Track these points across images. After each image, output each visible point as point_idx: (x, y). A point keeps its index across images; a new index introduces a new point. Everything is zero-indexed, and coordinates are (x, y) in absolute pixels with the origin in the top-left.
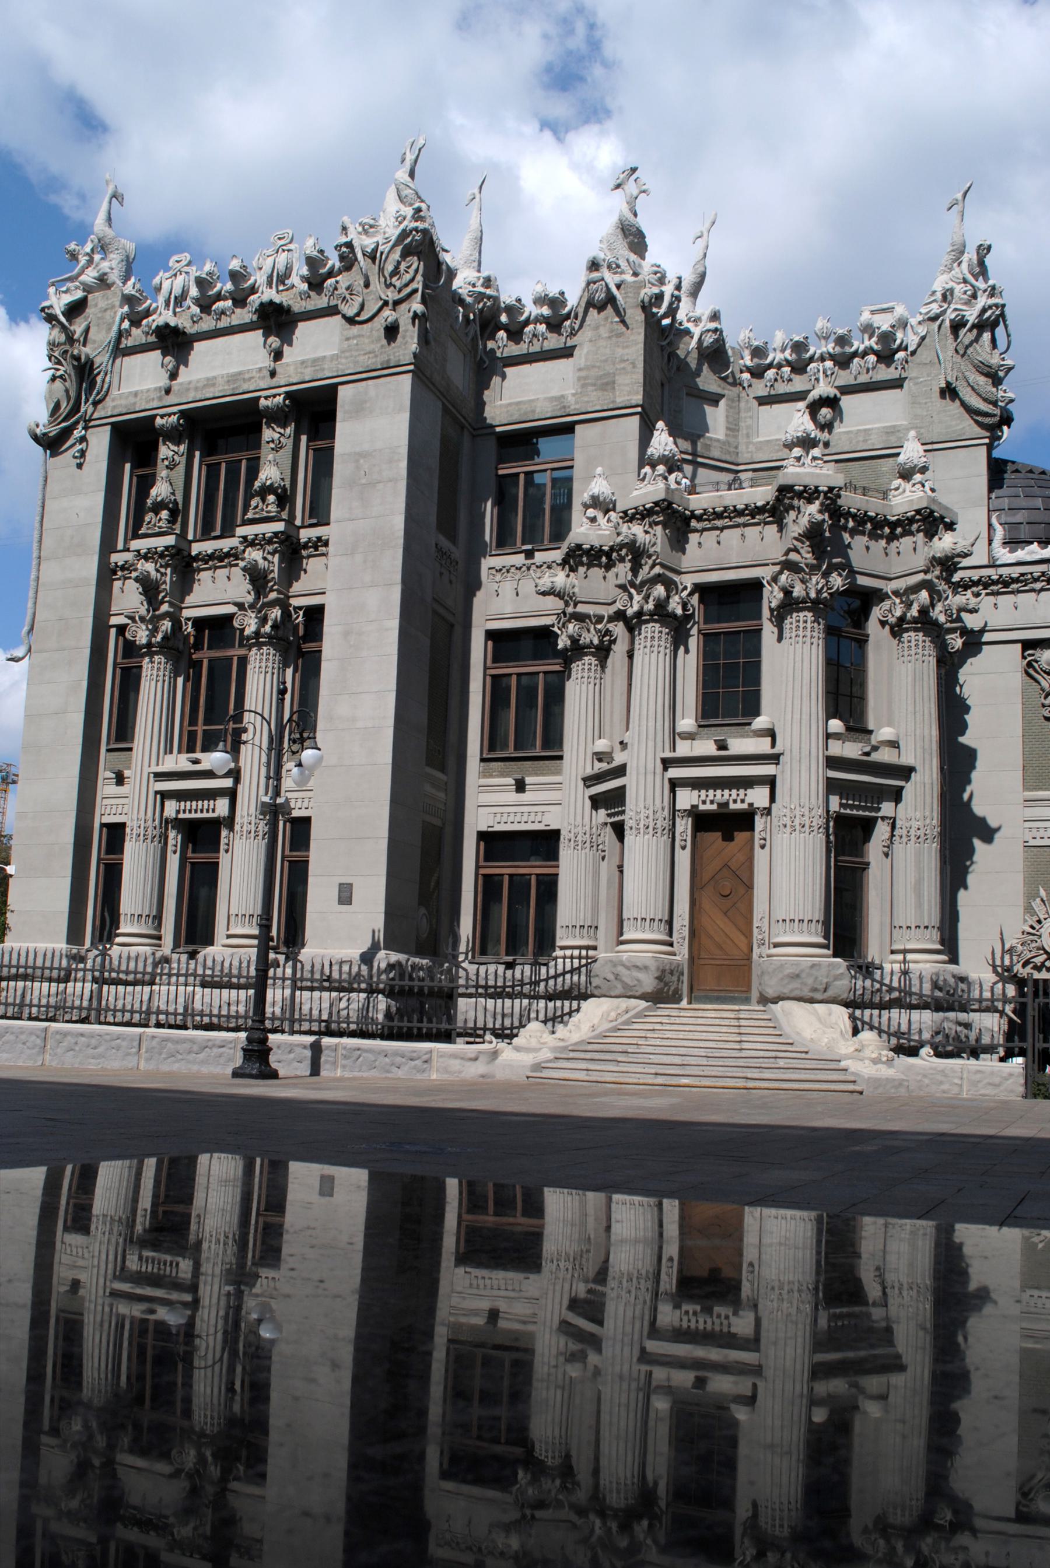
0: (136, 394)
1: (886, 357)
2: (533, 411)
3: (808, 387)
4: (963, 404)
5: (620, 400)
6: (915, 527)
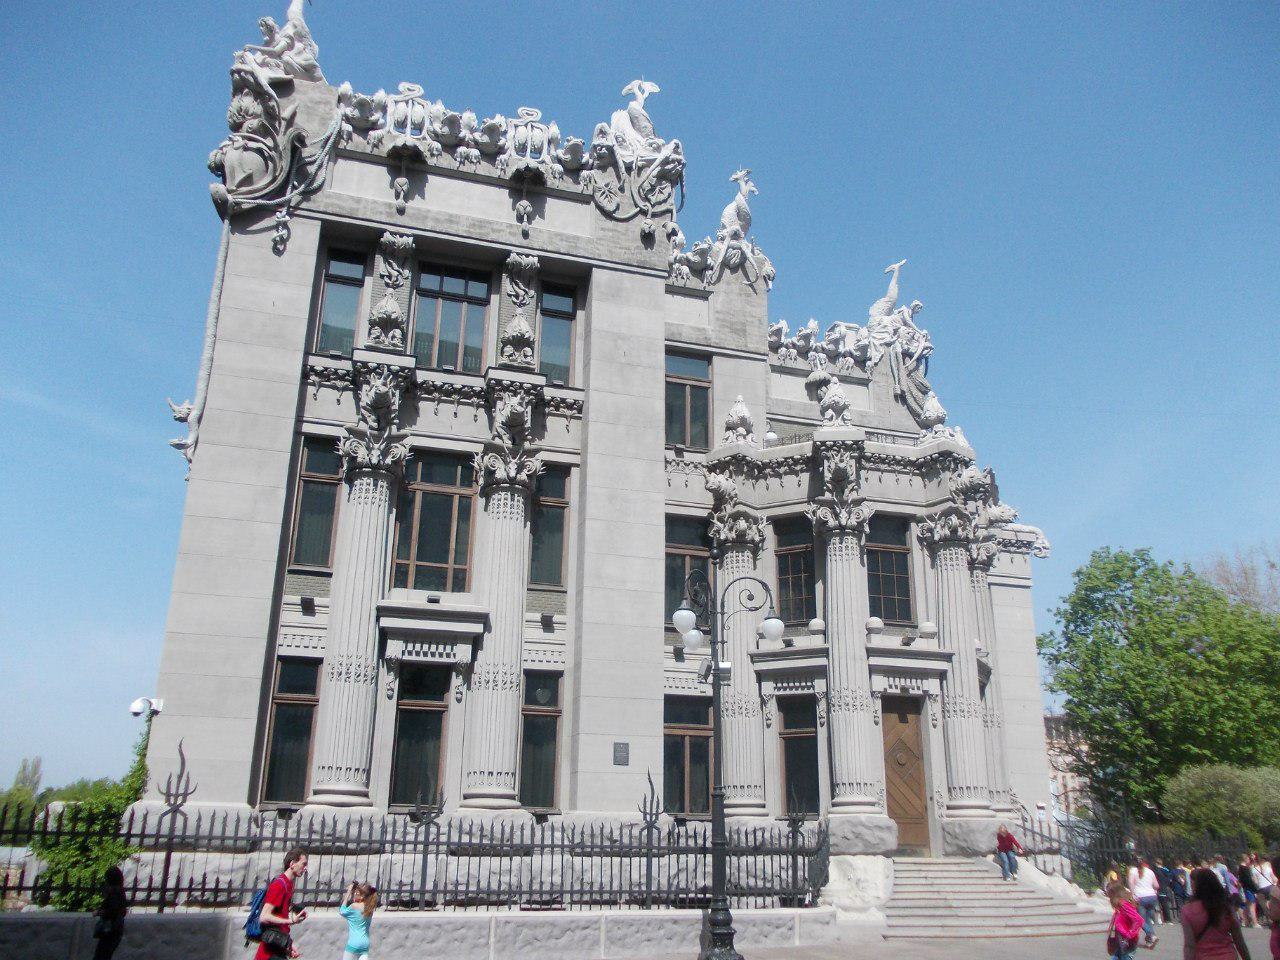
0: (358, 201)
1: (804, 353)
2: (680, 334)
3: (808, 368)
4: (910, 409)
5: (751, 347)
6: (979, 495)
